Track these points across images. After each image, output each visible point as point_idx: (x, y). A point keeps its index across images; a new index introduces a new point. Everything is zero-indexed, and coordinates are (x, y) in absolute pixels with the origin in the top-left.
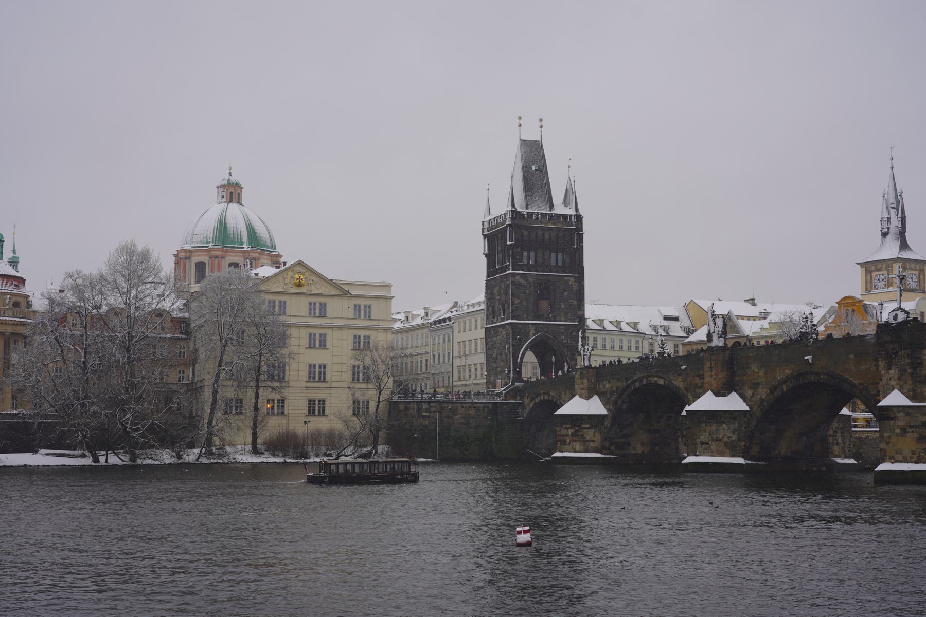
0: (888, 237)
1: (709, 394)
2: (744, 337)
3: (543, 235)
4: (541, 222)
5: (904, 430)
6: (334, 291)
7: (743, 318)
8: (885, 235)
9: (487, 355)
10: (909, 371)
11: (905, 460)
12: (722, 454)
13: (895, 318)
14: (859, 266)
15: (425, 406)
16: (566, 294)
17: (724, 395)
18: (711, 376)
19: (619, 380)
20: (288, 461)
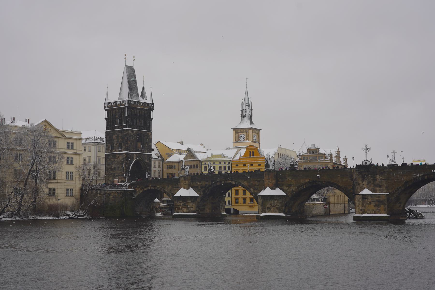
0: (246, 118)
1: (268, 189)
2: (198, 160)
3: (139, 112)
4: (139, 106)
5: (370, 203)
6: (59, 135)
7: (196, 152)
8: (243, 117)
9: (106, 167)
10: (372, 182)
11: (371, 213)
12: (275, 212)
13: (366, 163)
14: (232, 130)
15: (99, 192)
16: (148, 140)
17: (275, 189)
18: (269, 181)
19: (207, 181)
20: (54, 218)
